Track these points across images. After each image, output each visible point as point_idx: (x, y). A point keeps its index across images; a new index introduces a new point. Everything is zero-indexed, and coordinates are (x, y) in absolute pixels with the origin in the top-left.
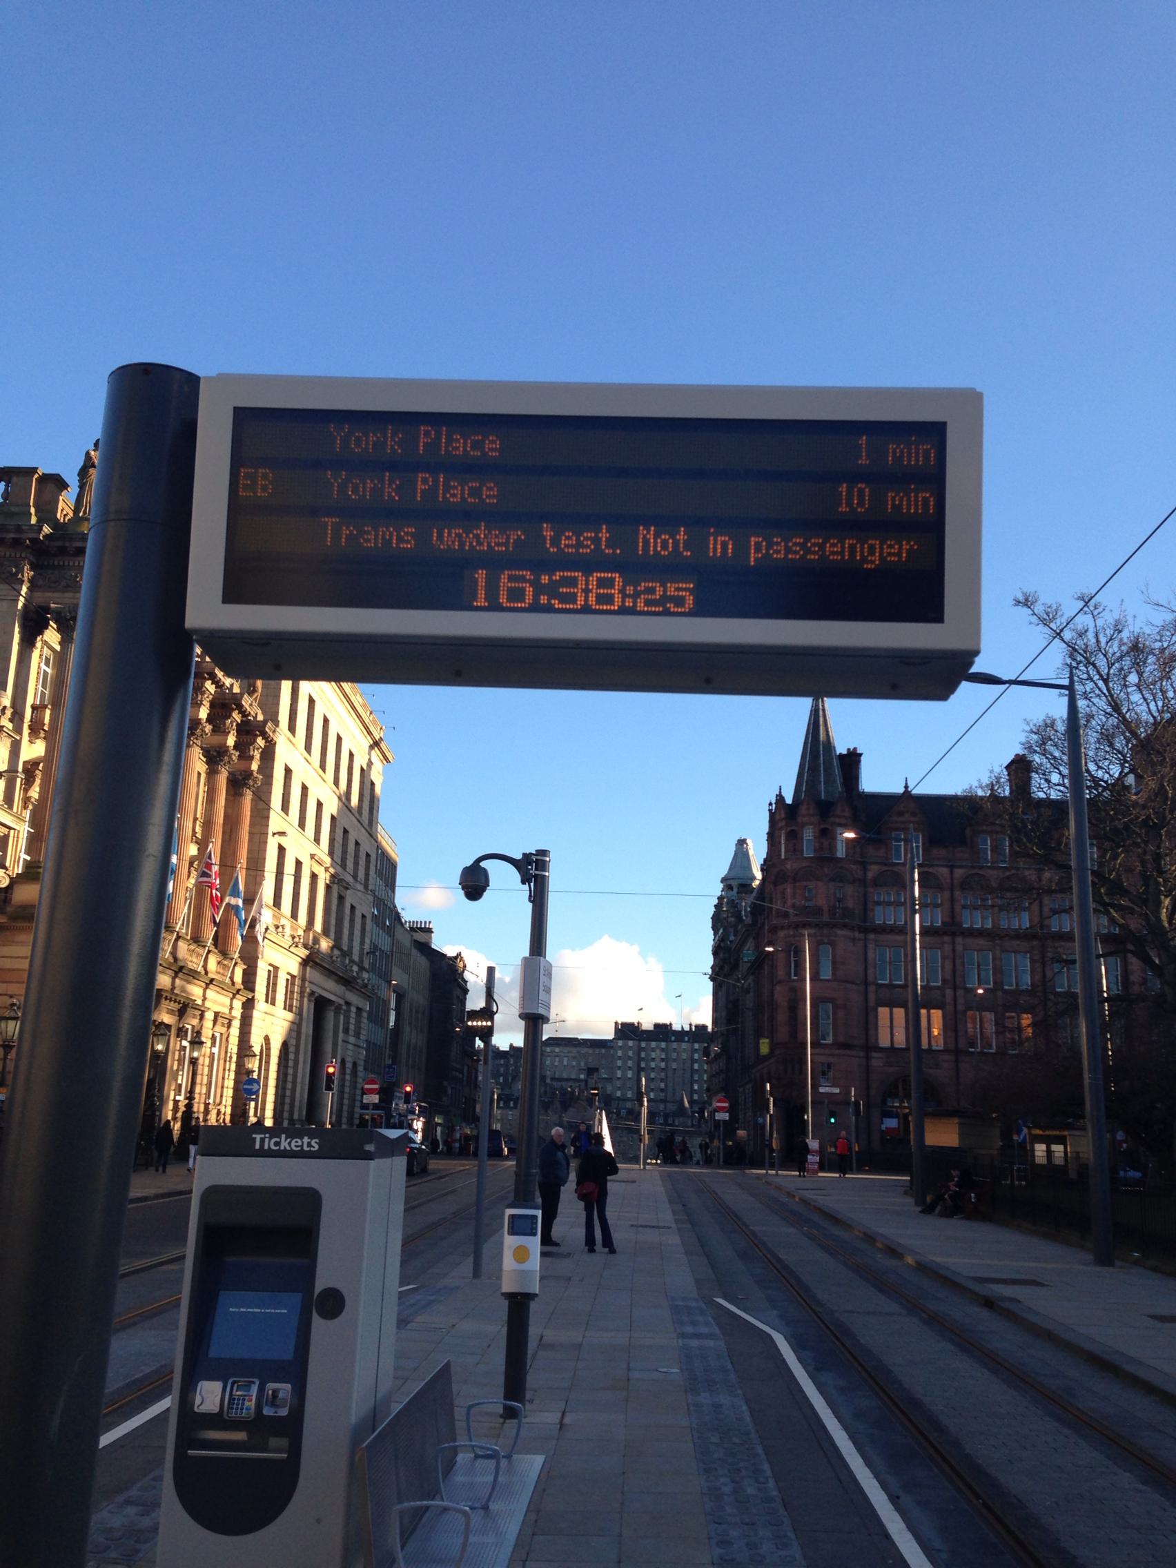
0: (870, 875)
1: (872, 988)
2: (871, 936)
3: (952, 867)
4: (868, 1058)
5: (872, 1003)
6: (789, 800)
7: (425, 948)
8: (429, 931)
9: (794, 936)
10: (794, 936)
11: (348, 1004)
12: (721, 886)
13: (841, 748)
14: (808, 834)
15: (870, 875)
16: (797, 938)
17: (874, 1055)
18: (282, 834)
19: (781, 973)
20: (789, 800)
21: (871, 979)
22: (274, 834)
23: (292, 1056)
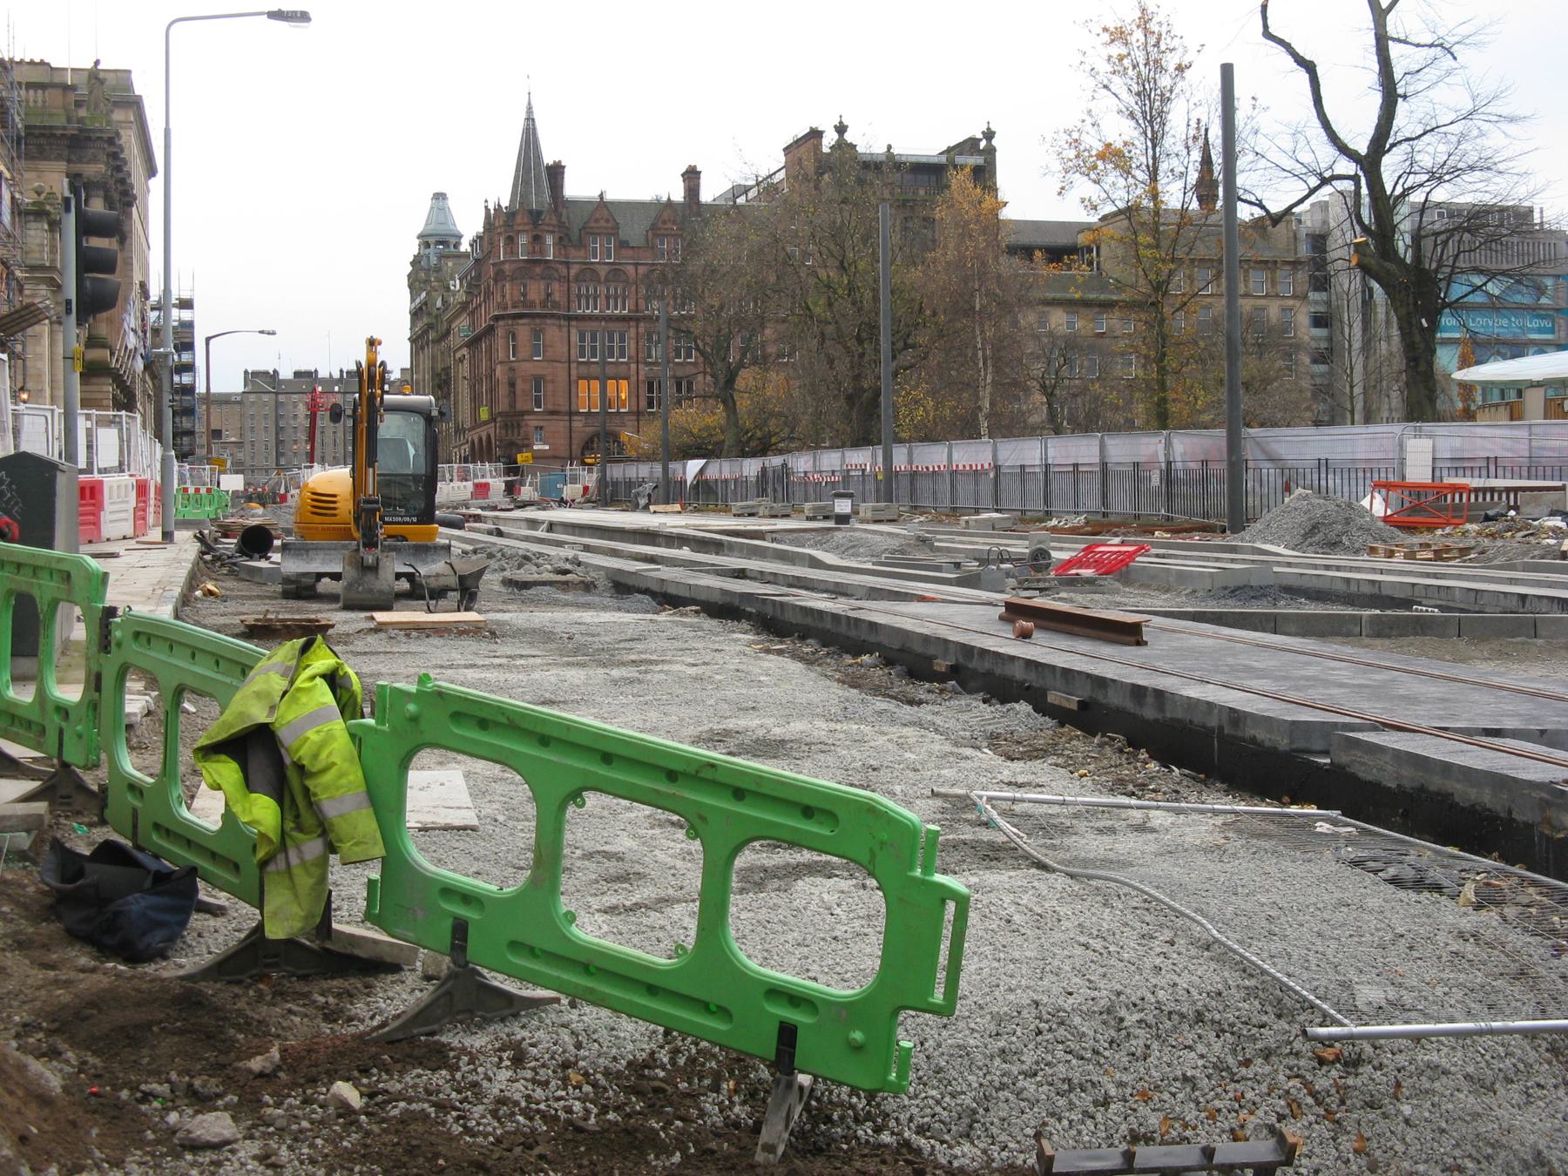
0: (573, 272)
1: (574, 366)
2: (574, 323)
3: (636, 265)
4: (570, 421)
5: (574, 378)
13: (548, 159)
14: (523, 240)
15: (573, 272)
17: (576, 418)
19: (501, 355)
21: (573, 357)
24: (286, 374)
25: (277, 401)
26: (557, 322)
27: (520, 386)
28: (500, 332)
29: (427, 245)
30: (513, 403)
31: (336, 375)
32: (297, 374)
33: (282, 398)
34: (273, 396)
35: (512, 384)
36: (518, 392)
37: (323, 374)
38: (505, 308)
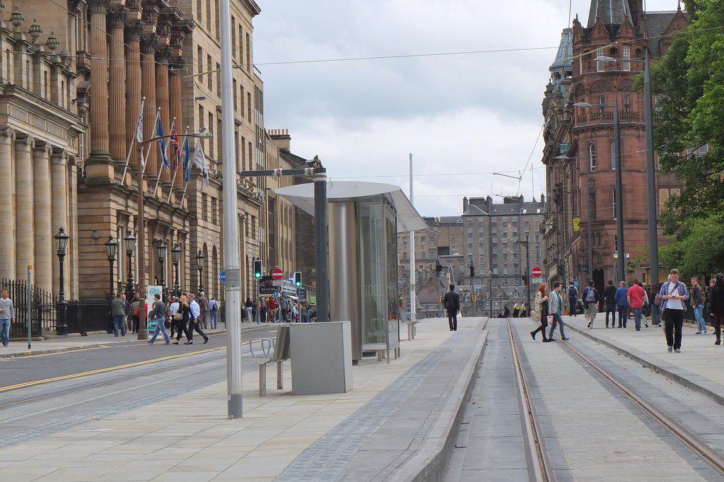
6: (585, 25)
7: (285, 153)
8: (287, 138)
9: (592, 137)
10: (592, 137)
11: (247, 214)
12: (550, 73)
16: (594, 139)
18: (202, 98)
20: (585, 25)
22: (197, 99)
23: (218, 256)
24: (498, 201)
25: (490, 222)
26: (635, 132)
27: (600, 196)
28: (581, 145)
29: (557, 76)
30: (593, 215)
31: (539, 200)
32: (507, 200)
33: (494, 220)
34: (487, 218)
35: (593, 195)
36: (598, 202)
37: (528, 199)
38: (585, 120)
